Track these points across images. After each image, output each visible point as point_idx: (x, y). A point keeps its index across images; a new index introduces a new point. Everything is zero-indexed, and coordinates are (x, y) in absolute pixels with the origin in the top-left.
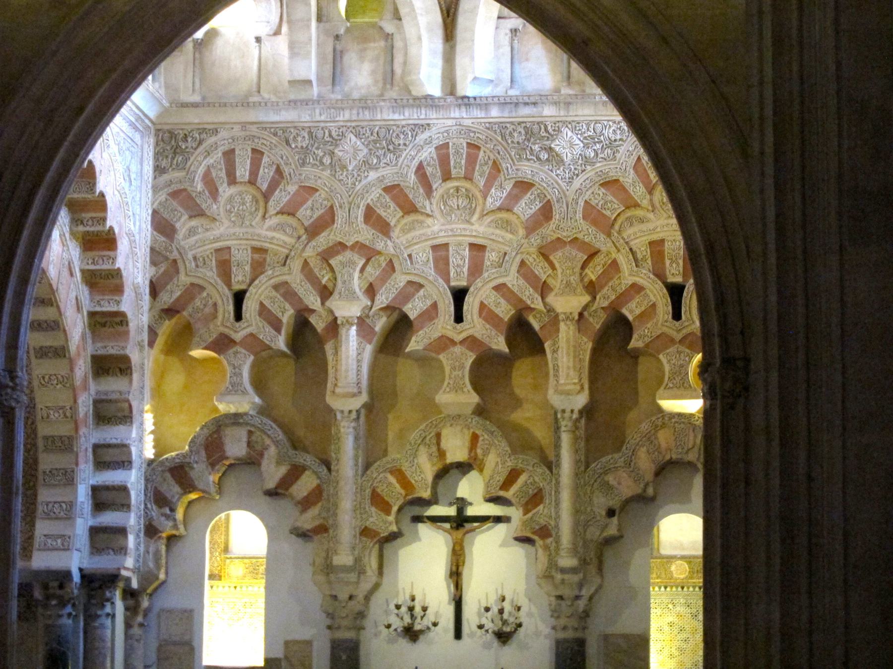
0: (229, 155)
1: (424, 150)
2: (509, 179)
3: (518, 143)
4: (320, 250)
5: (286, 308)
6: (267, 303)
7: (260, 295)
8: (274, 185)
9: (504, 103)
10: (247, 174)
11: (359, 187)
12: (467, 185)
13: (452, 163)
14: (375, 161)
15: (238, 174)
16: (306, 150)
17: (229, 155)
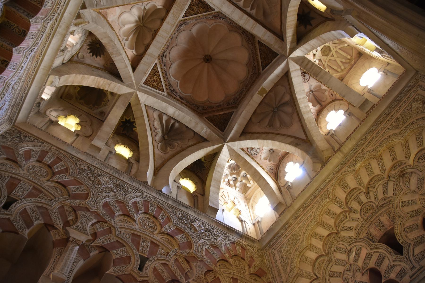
0: (44, 153)
1: (138, 198)
2: (174, 225)
3: (178, 216)
4: (74, 205)
5: (40, 219)
6: (29, 211)
7: (27, 206)
8: (60, 172)
9: (176, 201)
10: (50, 162)
11: (104, 194)
12: (154, 220)
13: (150, 208)
14: (115, 190)
15: (45, 159)
16: (83, 171)
17: (44, 153)
